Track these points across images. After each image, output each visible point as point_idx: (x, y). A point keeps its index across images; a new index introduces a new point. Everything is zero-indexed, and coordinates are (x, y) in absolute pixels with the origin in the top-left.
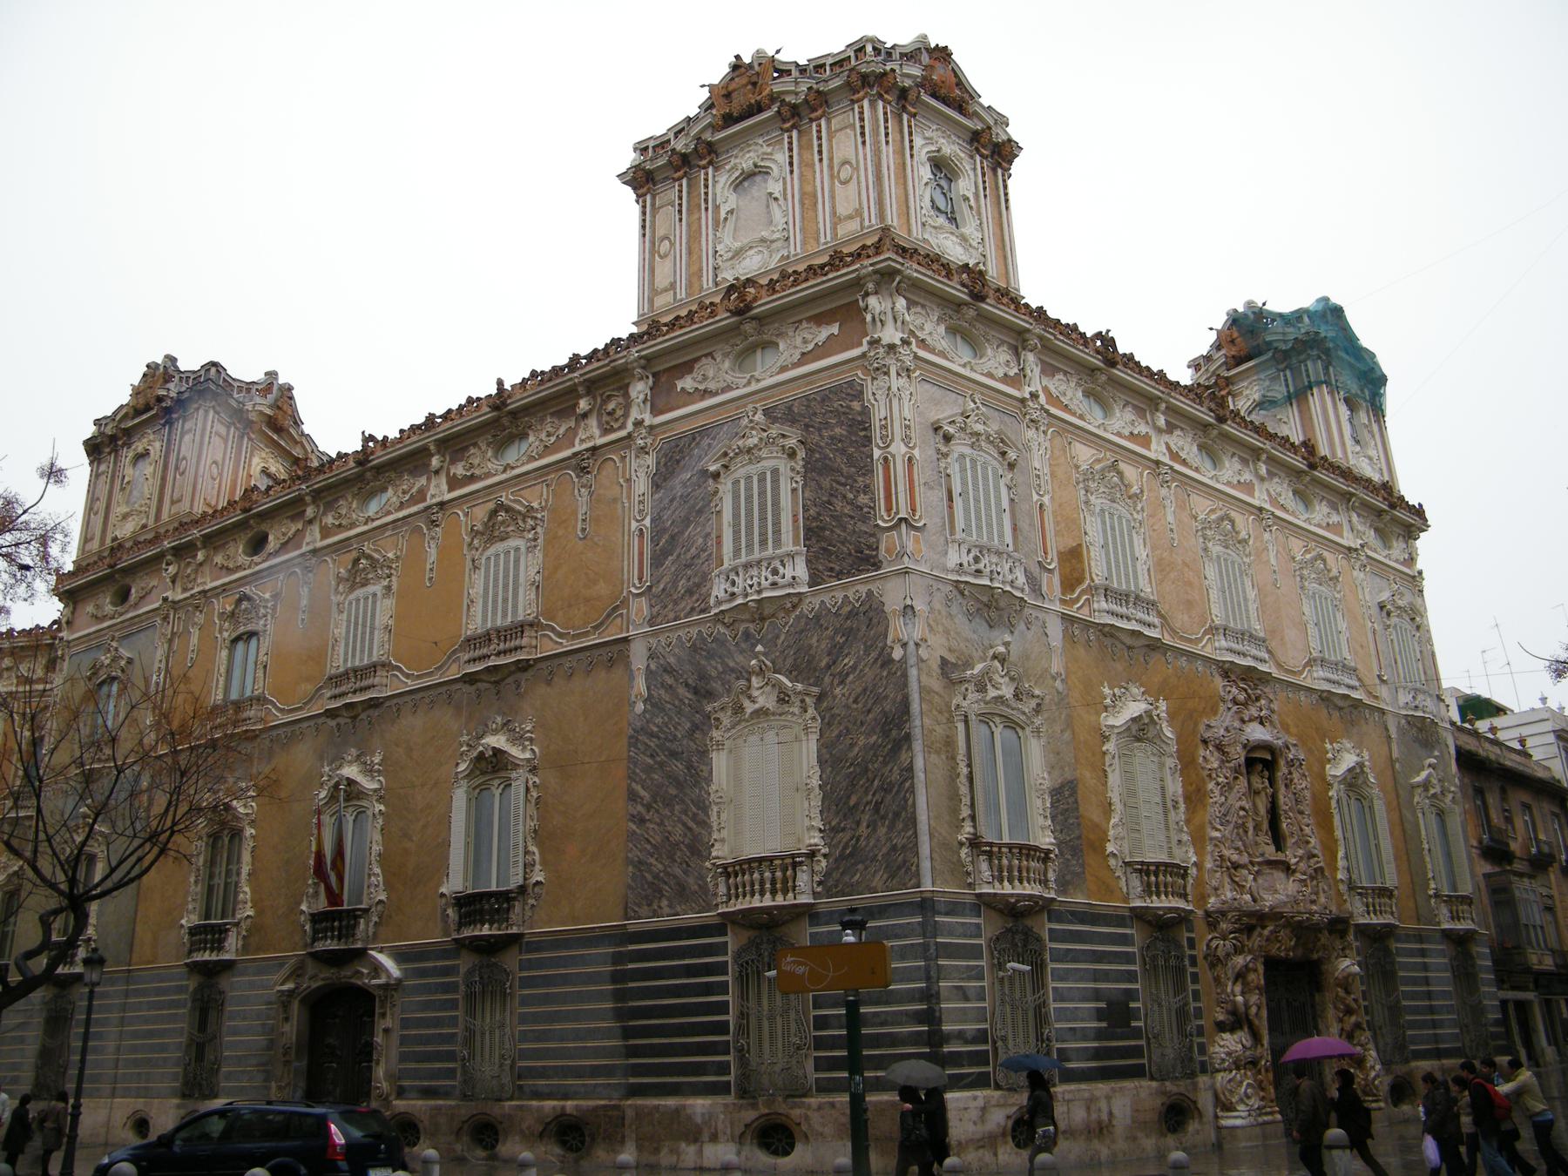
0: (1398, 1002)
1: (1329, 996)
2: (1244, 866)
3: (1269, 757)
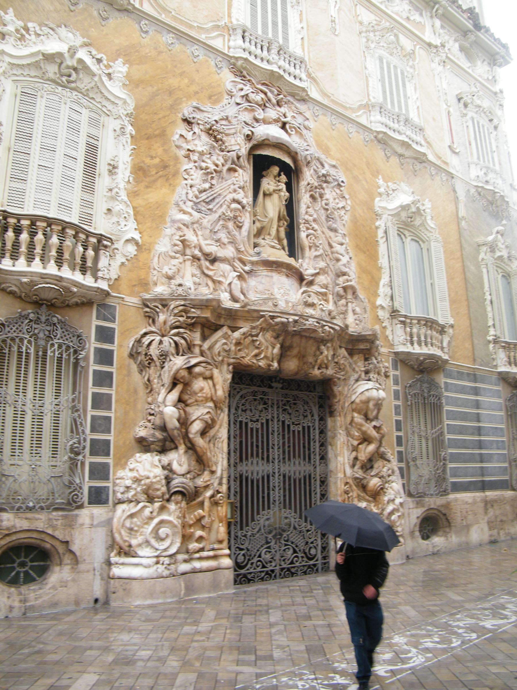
0: (442, 434)
1: (340, 420)
2: (224, 260)
3: (288, 160)
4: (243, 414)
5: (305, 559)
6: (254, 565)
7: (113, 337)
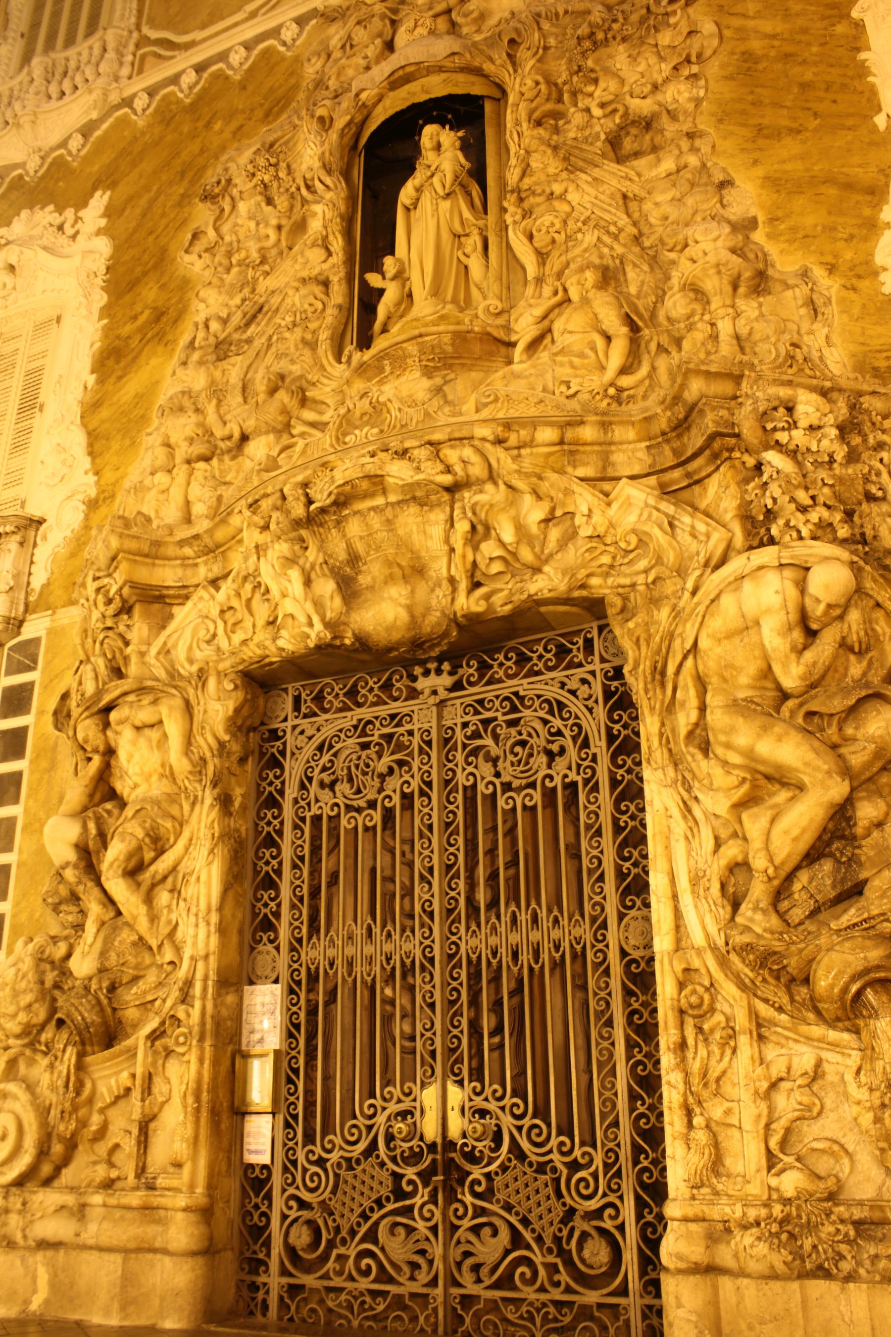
4: (326, 796)
5: (564, 1277)
6: (351, 1261)
7: (30, 699)
